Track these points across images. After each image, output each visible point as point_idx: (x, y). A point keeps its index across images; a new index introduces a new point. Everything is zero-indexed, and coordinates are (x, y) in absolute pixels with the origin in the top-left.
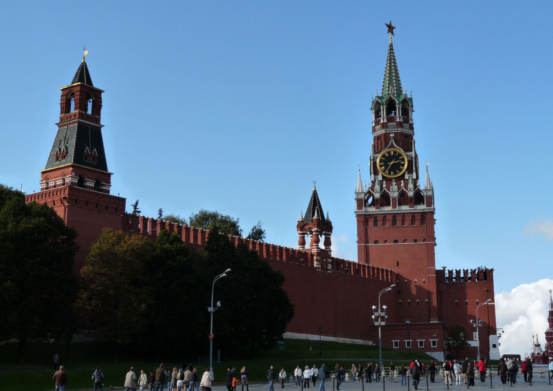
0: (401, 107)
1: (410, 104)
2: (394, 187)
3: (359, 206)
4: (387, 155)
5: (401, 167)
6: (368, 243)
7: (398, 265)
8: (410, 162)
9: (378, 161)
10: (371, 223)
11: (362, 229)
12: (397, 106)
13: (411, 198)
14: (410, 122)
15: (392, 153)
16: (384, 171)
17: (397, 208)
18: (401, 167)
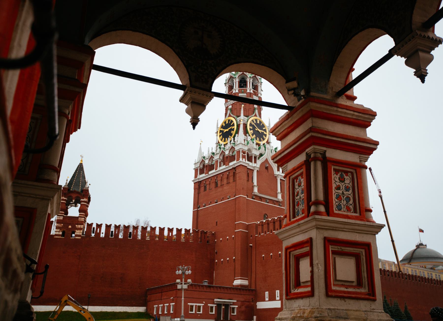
0: (237, 80)
1: (248, 77)
2: (219, 150)
3: (196, 176)
4: (224, 125)
5: (232, 132)
6: (199, 208)
7: (217, 225)
8: (238, 126)
9: (219, 132)
10: (202, 189)
11: (197, 196)
12: (234, 81)
13: (227, 157)
14: (248, 91)
15: (227, 123)
16: (222, 140)
17: (218, 170)
18: (232, 132)
